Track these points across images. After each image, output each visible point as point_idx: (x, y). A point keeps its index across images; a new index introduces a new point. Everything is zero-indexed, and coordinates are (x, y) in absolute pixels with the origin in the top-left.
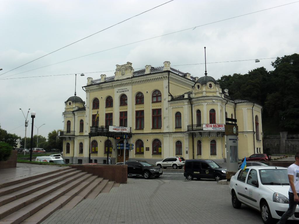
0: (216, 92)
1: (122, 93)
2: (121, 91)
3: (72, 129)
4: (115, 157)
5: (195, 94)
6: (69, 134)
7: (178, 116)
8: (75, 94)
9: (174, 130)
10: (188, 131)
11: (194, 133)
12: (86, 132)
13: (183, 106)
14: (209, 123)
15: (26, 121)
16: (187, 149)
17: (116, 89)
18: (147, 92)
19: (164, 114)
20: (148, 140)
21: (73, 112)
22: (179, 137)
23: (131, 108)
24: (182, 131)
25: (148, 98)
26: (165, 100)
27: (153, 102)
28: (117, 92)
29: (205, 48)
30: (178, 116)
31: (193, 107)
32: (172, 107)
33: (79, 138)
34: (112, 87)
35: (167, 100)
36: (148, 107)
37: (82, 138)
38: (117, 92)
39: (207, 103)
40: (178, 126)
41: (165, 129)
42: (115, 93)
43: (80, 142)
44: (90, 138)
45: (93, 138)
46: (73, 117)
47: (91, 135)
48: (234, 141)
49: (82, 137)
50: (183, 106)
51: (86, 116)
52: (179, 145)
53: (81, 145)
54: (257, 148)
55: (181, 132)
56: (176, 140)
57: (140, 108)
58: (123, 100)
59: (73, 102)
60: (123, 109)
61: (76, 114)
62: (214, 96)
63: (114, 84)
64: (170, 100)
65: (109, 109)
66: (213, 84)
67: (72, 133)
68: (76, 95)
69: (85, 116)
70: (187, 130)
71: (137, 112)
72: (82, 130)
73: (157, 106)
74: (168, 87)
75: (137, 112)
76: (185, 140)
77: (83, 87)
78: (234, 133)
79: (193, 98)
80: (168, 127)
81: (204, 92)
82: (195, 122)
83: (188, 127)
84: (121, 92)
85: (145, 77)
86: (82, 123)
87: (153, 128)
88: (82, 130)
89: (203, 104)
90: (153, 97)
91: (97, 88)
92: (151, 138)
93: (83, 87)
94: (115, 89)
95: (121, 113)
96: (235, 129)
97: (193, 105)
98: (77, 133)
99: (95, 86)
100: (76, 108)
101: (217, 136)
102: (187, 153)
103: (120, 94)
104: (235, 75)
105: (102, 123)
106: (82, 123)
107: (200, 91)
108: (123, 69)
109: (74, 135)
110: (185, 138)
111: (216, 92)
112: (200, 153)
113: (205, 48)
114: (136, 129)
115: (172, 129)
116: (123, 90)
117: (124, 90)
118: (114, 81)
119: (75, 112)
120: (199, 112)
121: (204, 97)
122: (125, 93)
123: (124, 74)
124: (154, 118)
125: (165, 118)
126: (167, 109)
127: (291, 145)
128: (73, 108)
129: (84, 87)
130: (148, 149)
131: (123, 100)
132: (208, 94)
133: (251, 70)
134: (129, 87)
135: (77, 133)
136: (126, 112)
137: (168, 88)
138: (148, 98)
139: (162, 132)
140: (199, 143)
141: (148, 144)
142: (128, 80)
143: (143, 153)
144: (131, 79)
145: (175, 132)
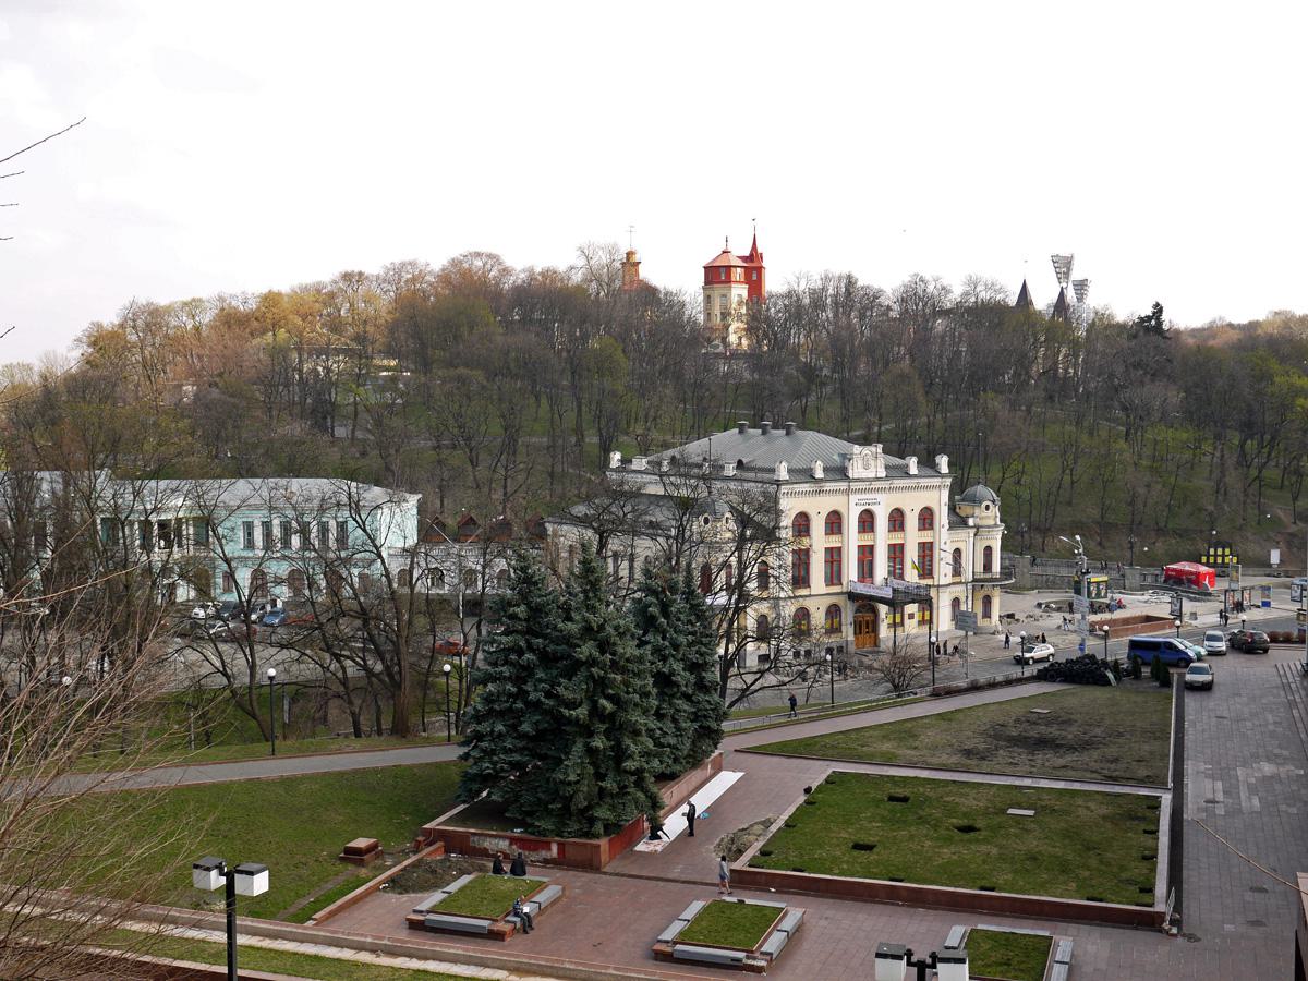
1: (867, 507)
7: (957, 552)
9: (949, 580)
17: (854, 498)
22: (959, 591)
25: (912, 521)
30: (957, 552)
34: (848, 492)
36: (912, 537)
40: (957, 572)
42: (852, 504)
55: (961, 583)
56: (953, 596)
58: (867, 521)
63: (854, 485)
65: (834, 538)
70: (971, 579)
73: (927, 537)
99: (806, 485)
126: (945, 543)
131: (867, 521)
136: (871, 548)
138: (912, 521)
139: (936, 584)
143: (902, 624)
145: (954, 584)
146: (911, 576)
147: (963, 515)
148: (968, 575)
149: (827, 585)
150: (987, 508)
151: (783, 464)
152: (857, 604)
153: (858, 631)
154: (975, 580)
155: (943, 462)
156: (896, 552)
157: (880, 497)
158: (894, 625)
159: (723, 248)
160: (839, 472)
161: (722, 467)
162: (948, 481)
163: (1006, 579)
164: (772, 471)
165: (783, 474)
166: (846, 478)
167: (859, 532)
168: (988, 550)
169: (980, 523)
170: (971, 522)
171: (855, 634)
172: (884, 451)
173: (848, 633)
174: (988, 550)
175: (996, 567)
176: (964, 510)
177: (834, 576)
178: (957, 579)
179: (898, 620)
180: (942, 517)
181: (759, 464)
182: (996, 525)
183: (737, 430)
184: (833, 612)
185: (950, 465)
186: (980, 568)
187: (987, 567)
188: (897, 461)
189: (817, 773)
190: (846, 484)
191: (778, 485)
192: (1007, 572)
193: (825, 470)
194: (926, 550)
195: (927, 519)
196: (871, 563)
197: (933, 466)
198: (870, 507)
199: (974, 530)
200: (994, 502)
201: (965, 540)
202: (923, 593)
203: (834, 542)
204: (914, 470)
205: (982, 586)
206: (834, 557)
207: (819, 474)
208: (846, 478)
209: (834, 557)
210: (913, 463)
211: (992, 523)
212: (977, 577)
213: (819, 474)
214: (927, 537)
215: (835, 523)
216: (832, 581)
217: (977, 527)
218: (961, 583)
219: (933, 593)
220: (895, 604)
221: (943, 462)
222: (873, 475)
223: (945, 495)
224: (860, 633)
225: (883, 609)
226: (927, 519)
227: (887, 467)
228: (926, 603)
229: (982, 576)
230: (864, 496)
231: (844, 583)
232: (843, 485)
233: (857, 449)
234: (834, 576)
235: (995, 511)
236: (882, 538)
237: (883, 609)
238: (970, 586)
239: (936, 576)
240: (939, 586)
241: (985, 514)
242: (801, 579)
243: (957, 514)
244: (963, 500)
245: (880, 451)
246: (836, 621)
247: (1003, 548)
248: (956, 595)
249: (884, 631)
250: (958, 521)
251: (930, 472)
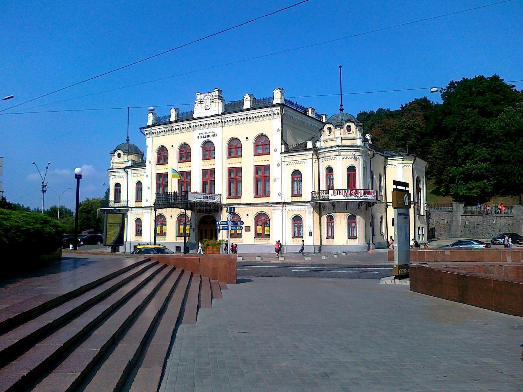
0: (355, 139)
1: (207, 138)
2: (205, 135)
3: (123, 196)
4: (196, 242)
5: (325, 141)
6: (117, 205)
7: (297, 175)
8: (128, 140)
9: (290, 199)
10: (312, 200)
11: (322, 203)
12: (147, 201)
14: (345, 187)
15: (43, 182)
16: (311, 230)
17: (196, 133)
18: (247, 138)
19: (274, 173)
20: (247, 215)
21: (125, 168)
22: (296, 210)
26: (275, 150)
27: (256, 155)
28: (198, 137)
29: (340, 67)
30: (297, 175)
31: (320, 162)
32: (286, 163)
33: (134, 211)
35: (279, 151)
37: (139, 211)
38: (198, 137)
39: (342, 157)
40: (297, 192)
41: (274, 197)
43: (136, 217)
44: (155, 211)
45: (159, 211)
46: (125, 177)
47: (157, 206)
48: (405, 216)
49: (141, 209)
51: (147, 176)
52: (297, 220)
53: (138, 221)
54: (419, 228)
57: (234, 163)
59: (124, 153)
60: (208, 165)
61: (129, 173)
62: (355, 145)
63: (193, 123)
64: (283, 151)
65: (185, 164)
66: (353, 126)
67: (123, 204)
68: (129, 141)
69: (145, 175)
70: (310, 199)
71: (230, 170)
72: (139, 198)
73: (262, 160)
74: (280, 129)
75: (230, 170)
76: (307, 214)
77: (141, 129)
78: (405, 204)
79: (321, 149)
80: (280, 194)
81: (338, 138)
82: (324, 187)
83: (312, 194)
84: (204, 137)
85: (244, 113)
86: (139, 186)
87: (256, 196)
88: (139, 198)
89: (337, 157)
90: (256, 146)
91: (165, 130)
92: (254, 211)
93: (141, 129)
95: (205, 172)
96: (406, 199)
98: (132, 203)
100: (130, 163)
101: (359, 209)
102: (310, 234)
103: (203, 140)
104: (380, 110)
105: (173, 187)
106: (139, 186)
107: (332, 136)
108: (207, 100)
109: (127, 207)
110: (307, 212)
111: (355, 139)
113: (340, 67)
114: (230, 196)
115: (288, 197)
116: (208, 134)
117: (209, 134)
118: (193, 119)
119: (129, 170)
120: (330, 170)
121: (339, 146)
122: (211, 139)
123: (209, 108)
124: (257, 181)
125: (275, 180)
126: (278, 165)
127: (470, 222)
128: (125, 162)
129: (142, 128)
130: (248, 229)
132: (345, 142)
133: (406, 104)
134: (217, 130)
135: (132, 203)
136: (213, 171)
137: (280, 132)
140: (331, 219)
141: (249, 221)
142: (216, 118)
143: (240, 236)
144: (220, 117)
198: (209, 138)
223: (277, 122)
230: (201, 131)
248: (299, 213)
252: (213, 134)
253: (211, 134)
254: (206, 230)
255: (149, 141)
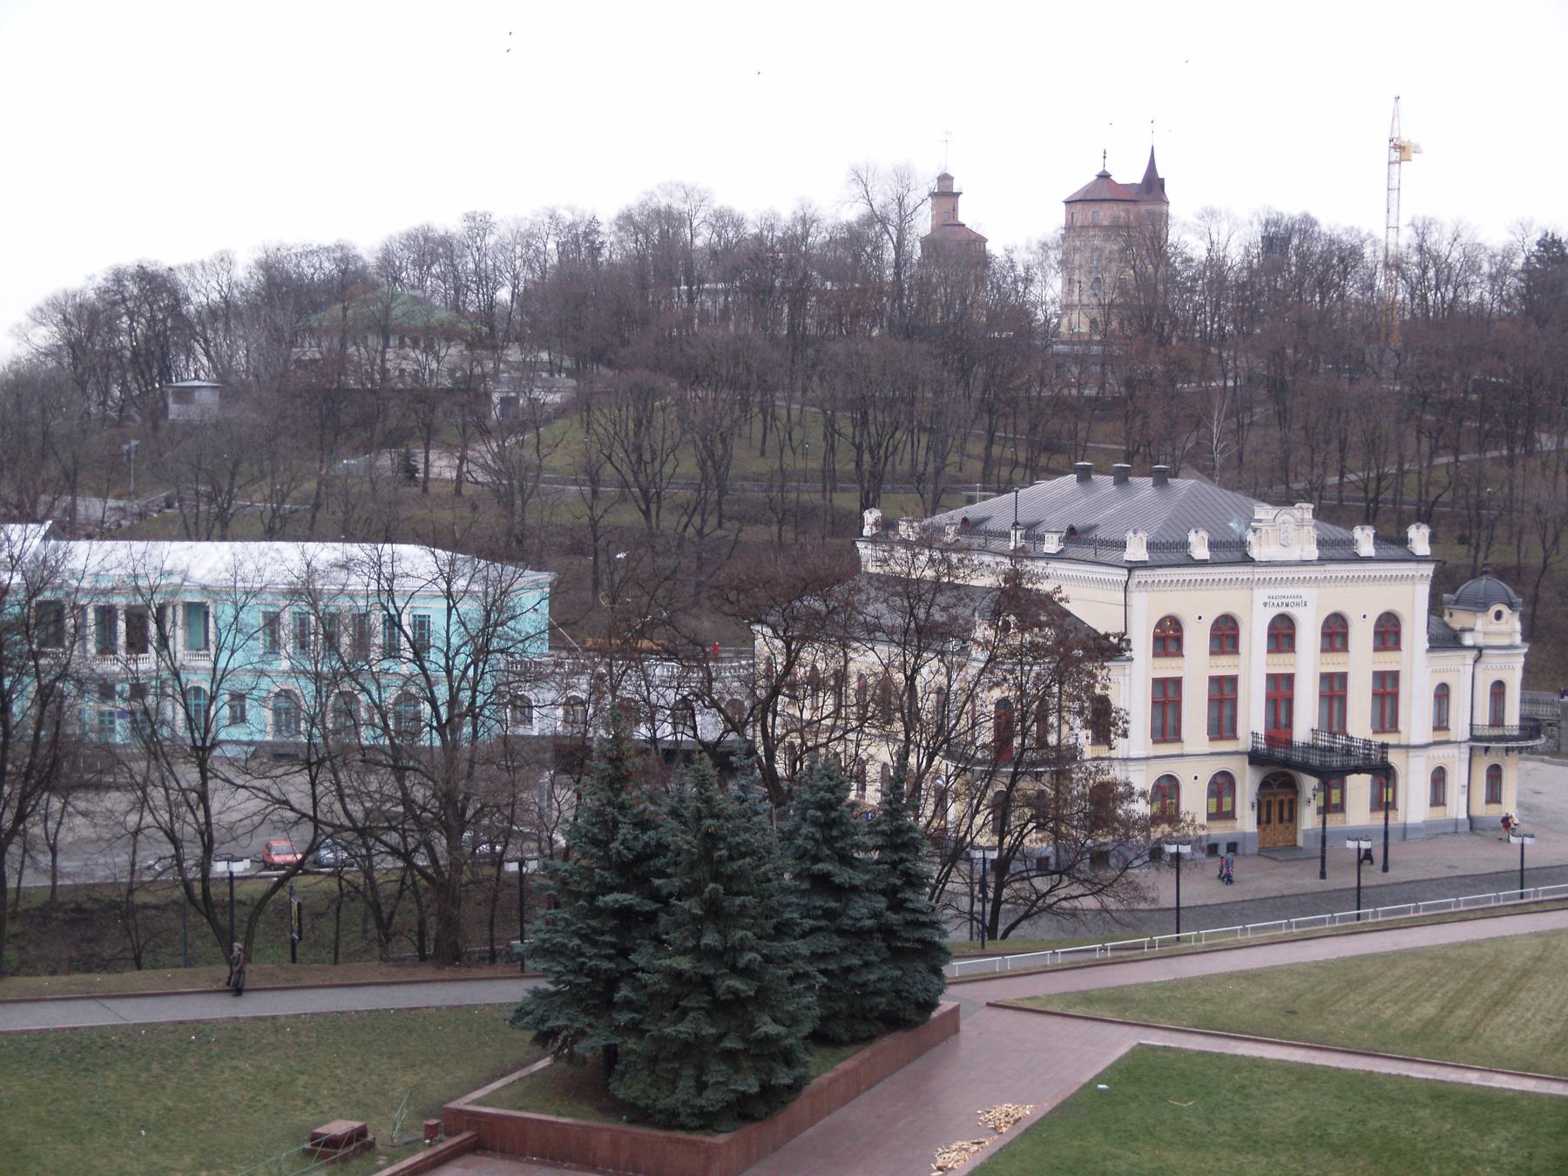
1: (1283, 610)
7: (1442, 694)
10: (1470, 740)
13: (1461, 668)
17: (1261, 594)
22: (1441, 756)
23: (1308, 663)
24: (1452, 739)
25: (1362, 634)
28: (1265, 604)
30: (1442, 694)
40: (1441, 724)
42: (1258, 606)
50: (1461, 668)
52: (1439, 777)
55: (1447, 742)
58: (1282, 634)
70: (1467, 736)
73: (1387, 661)
94: (1256, 591)
95: (1273, 679)
97: (1480, 667)
112: (1494, 797)
117: (1290, 601)
131: (1282, 634)
136: (1290, 678)
138: (1362, 634)
139: (1404, 742)
146: (1360, 723)
147: (1456, 626)
148: (1459, 728)
149: (1211, 739)
150: (1498, 615)
151: (1140, 534)
152: (1268, 770)
153: (1264, 818)
154: (1474, 738)
155: (1419, 538)
156: (1334, 689)
157: (1307, 593)
158: (1326, 809)
159: (1099, 170)
160: (1232, 552)
161: (1042, 539)
162: (1428, 569)
163: (1530, 738)
164: (1122, 545)
165: (1136, 550)
166: (1248, 561)
167: (1269, 651)
168: (1498, 689)
169: (1481, 641)
170: (1468, 640)
171: (1259, 822)
172: (1316, 515)
173: (1246, 821)
174: (1498, 689)
175: (1513, 717)
176: (1458, 620)
177: (1222, 723)
178: (1441, 736)
179: (1335, 799)
180: (1416, 630)
181: (1101, 534)
182: (1511, 647)
183: (1072, 478)
184: (1222, 785)
185: (1433, 540)
186: (1483, 717)
187: (1497, 719)
188: (1338, 532)
189: (1119, 1042)
190: (1248, 569)
191: (1130, 570)
192: (1531, 727)
193: (1212, 545)
194: (1387, 688)
195: (1388, 632)
196: (1290, 702)
197: (1404, 541)
199: (1475, 652)
200: (1511, 606)
201: (1456, 668)
202: (1376, 757)
203: (1224, 666)
204: (1366, 546)
205: (1487, 749)
206: (1223, 692)
207: (1200, 551)
208: (1248, 561)
209: (1223, 692)
210: (1365, 540)
211: (1505, 641)
212: (1478, 733)
213: (1200, 551)
214: (1387, 661)
215: (1226, 635)
216: (1163, 733)
217: (1479, 650)
218: (1447, 742)
219: (1394, 758)
220: (1332, 776)
221: (1419, 538)
222: (1296, 557)
223: (1423, 592)
224: (1268, 821)
225: (1309, 783)
226: (1388, 632)
227: (1321, 543)
228: (1384, 774)
229: (1487, 732)
231: (1241, 731)
232: (1243, 572)
233: (1263, 512)
234: (1222, 723)
235: (1512, 625)
236: (1308, 663)
237: (1309, 783)
238: (1465, 749)
239: (1401, 727)
240: (1408, 747)
241: (1496, 626)
242: (1167, 725)
243: (1446, 625)
244: (1457, 602)
245: (1309, 515)
246: (1227, 800)
247: (1525, 685)
249: (1309, 819)
250: (1445, 640)
251: (1394, 551)
252: (1298, 600)
253: (1295, 600)
254: (1269, 804)
255: (1138, 599)
